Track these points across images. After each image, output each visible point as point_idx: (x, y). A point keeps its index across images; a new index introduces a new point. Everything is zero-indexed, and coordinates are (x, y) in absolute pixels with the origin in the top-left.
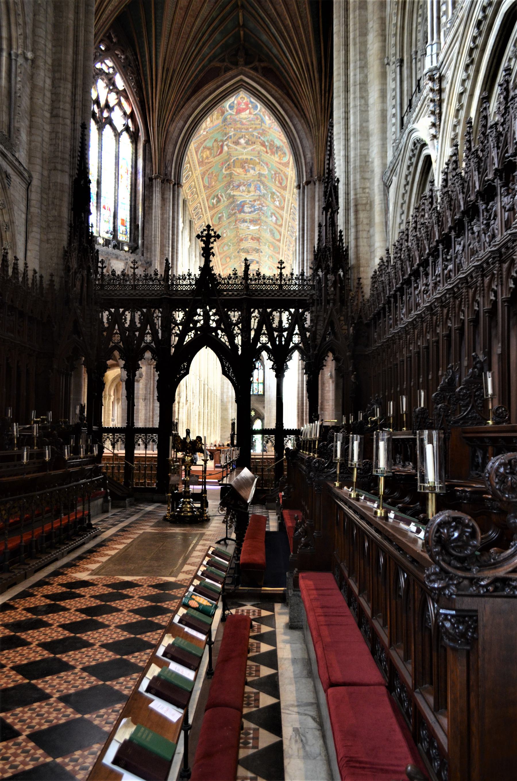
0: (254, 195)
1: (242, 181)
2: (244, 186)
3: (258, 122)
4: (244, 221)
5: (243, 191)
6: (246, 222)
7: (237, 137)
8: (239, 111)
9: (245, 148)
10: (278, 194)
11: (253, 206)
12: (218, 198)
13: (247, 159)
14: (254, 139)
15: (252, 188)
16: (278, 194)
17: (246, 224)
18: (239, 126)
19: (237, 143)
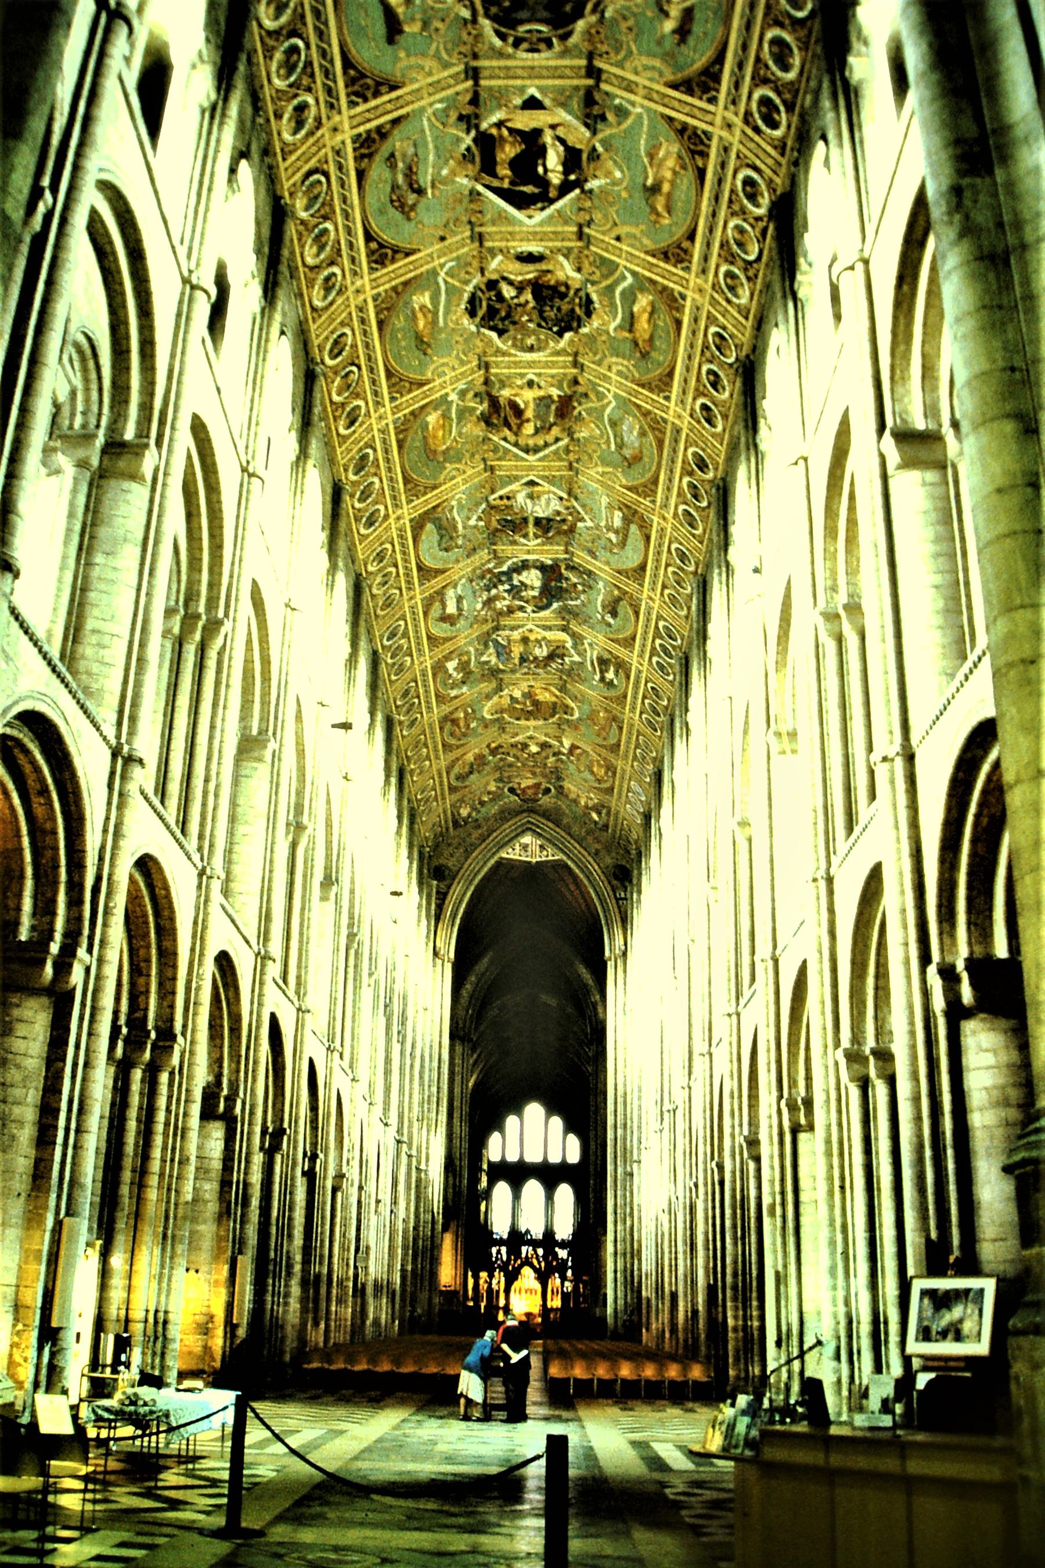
0: (513, 629)
1: (541, 671)
2: (536, 658)
3: (506, 774)
4: (544, 525)
5: (537, 641)
6: (538, 522)
7: (544, 754)
8: (537, 786)
9: (531, 738)
10: (454, 693)
11: (515, 591)
12: (601, 672)
13: (527, 719)
14: (513, 751)
15: (517, 650)
16: (454, 693)
17: (541, 511)
18: (538, 770)
19: (544, 746)
